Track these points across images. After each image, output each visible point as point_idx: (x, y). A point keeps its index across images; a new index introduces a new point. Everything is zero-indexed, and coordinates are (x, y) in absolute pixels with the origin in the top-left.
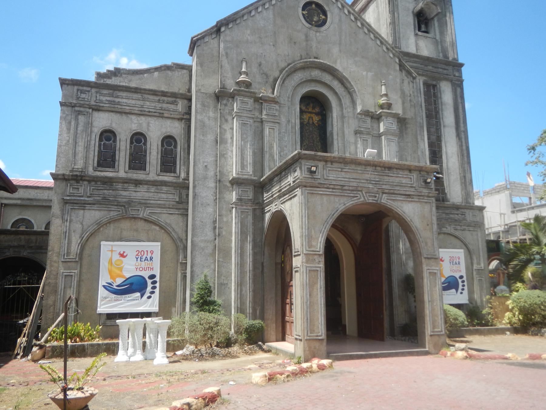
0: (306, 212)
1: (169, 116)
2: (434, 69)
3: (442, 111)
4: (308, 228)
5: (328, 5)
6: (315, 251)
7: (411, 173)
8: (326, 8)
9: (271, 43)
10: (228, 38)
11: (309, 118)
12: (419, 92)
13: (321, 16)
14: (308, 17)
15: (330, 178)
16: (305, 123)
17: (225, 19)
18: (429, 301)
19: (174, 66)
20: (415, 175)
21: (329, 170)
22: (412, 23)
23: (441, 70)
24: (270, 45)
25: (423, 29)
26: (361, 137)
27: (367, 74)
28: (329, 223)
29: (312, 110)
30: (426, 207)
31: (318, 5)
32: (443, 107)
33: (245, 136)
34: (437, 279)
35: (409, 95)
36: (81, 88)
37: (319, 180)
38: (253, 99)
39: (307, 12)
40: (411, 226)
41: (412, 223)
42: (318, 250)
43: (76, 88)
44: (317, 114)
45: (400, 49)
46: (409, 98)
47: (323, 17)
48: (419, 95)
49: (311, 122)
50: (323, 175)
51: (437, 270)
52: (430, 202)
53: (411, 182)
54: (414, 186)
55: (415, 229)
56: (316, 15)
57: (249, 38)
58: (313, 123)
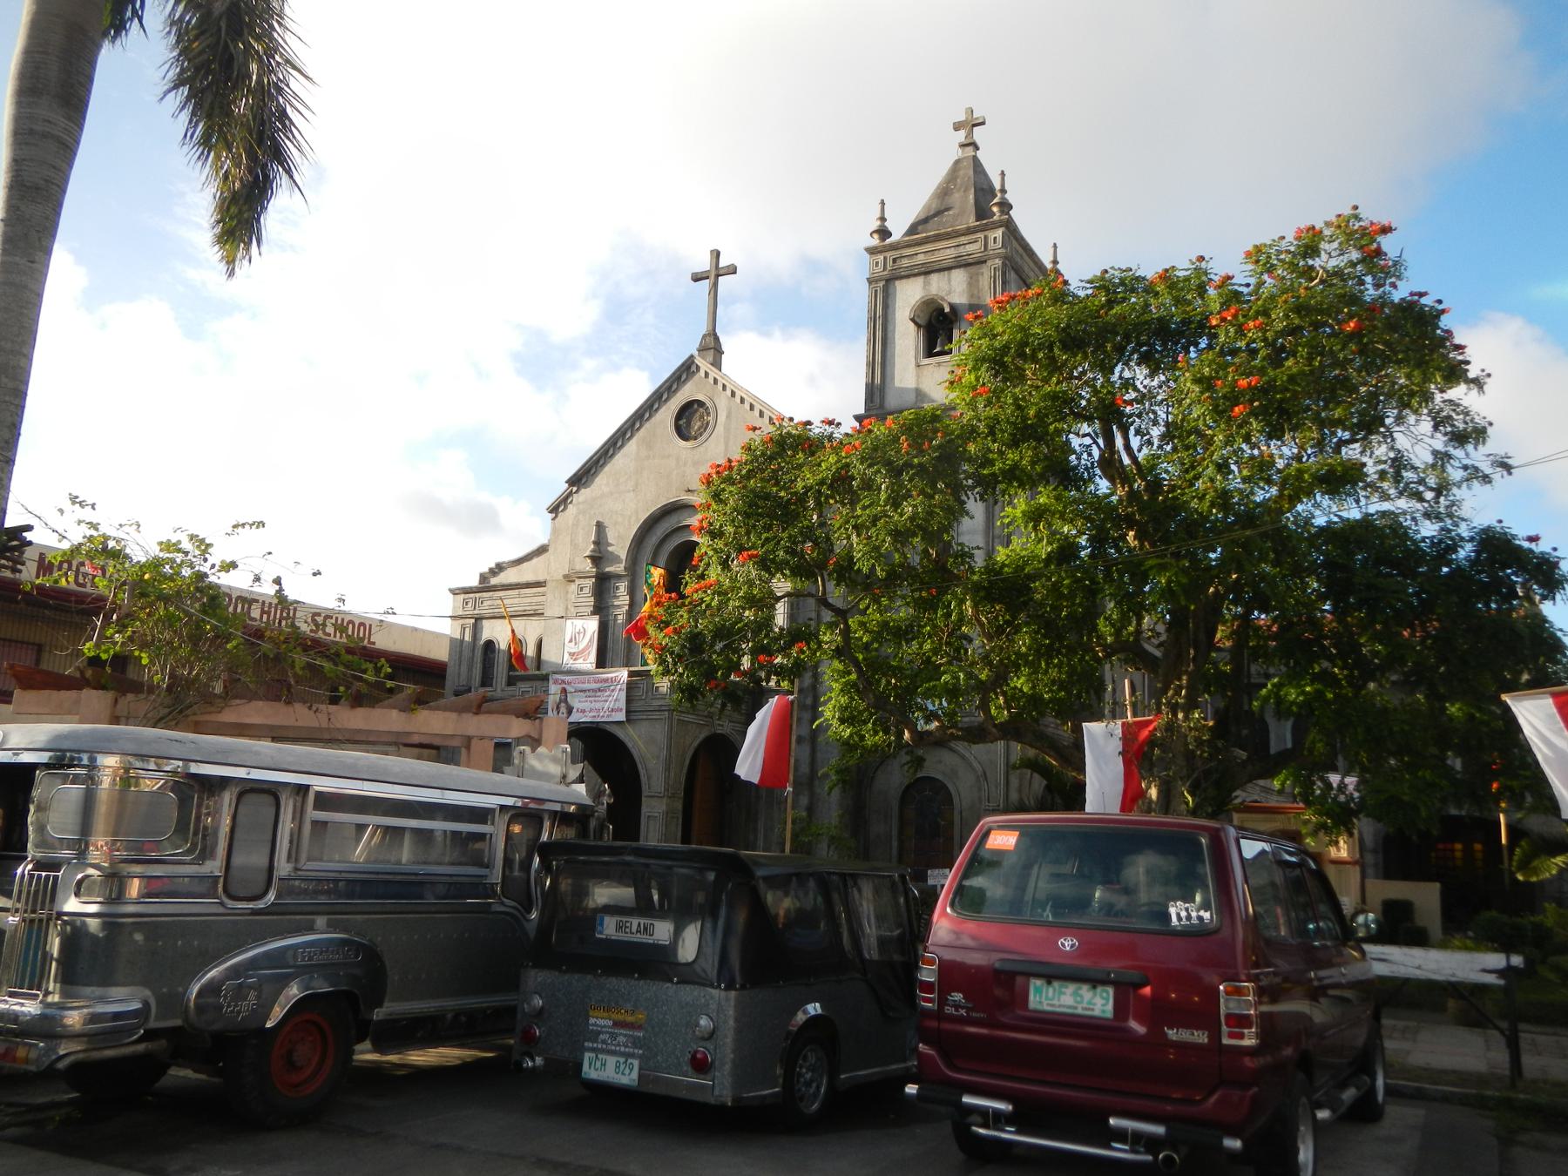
8: (708, 404)
17: (575, 475)
31: (701, 404)
36: (467, 596)
43: (462, 596)
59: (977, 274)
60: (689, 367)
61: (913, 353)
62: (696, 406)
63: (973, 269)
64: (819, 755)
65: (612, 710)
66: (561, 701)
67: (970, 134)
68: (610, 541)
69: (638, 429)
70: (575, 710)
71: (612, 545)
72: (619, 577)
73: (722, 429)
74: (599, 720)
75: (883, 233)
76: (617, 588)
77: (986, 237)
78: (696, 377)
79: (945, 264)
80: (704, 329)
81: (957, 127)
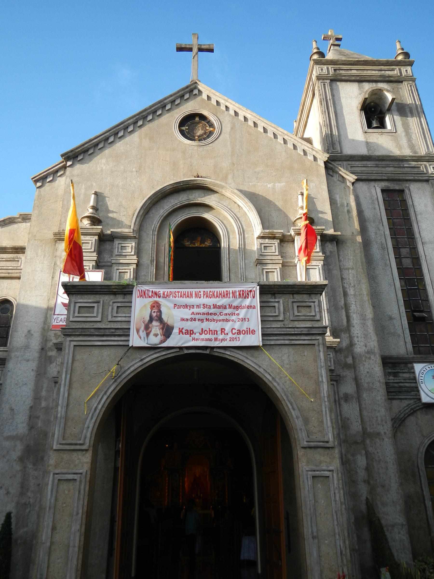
0: (68, 376)
1: (7, 275)
2: (397, 169)
4: (68, 405)
6: (76, 444)
7: (275, 298)
8: (212, 118)
9: (134, 169)
12: (376, 203)
13: (207, 128)
14: (188, 133)
15: (119, 319)
17: (72, 151)
18: (313, 538)
19: (21, 217)
20: (281, 302)
21: (118, 307)
23: (409, 170)
24: (132, 172)
26: (263, 269)
27: (274, 185)
28: (108, 393)
29: (200, 244)
30: (306, 353)
31: (202, 117)
32: (419, 217)
34: (332, 489)
37: (98, 324)
38: (96, 237)
39: (187, 127)
40: (274, 389)
41: (275, 384)
42: (81, 442)
45: (341, 152)
46: (346, 209)
47: (211, 129)
48: (377, 206)
50: (107, 316)
51: (332, 471)
52: (314, 344)
53: (275, 312)
54: (281, 319)
55: (283, 395)
56: (200, 129)
57: (104, 168)
59: (398, 89)
60: (192, 91)
61: (359, 125)
62: (197, 119)
63: (395, 85)
64: (365, 413)
65: (239, 332)
66: (151, 319)
68: (111, 209)
69: (140, 127)
70: (176, 331)
71: (113, 212)
72: (125, 238)
73: (228, 136)
74: (217, 344)
75: (321, 54)
76: (123, 248)
77: (400, 70)
78: (199, 98)
79: (375, 78)
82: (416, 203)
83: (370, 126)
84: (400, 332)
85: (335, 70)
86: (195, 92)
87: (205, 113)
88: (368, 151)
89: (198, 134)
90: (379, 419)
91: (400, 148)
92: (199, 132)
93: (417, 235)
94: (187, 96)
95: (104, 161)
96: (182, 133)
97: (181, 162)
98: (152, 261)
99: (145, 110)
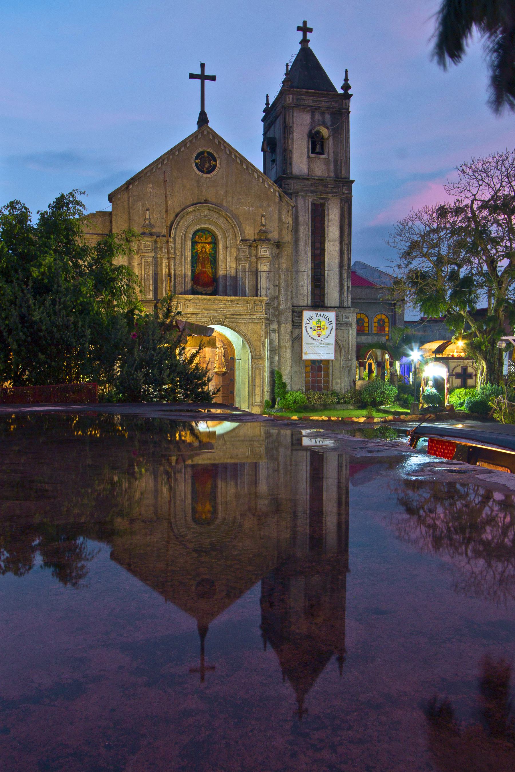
3: (328, 227)
5: (217, 153)
8: (215, 155)
10: (135, 193)
11: (202, 247)
14: (200, 165)
16: (199, 252)
22: (306, 146)
25: (318, 150)
32: (330, 223)
33: (147, 270)
35: (287, 223)
39: (199, 161)
44: (209, 243)
47: (214, 163)
48: (307, 215)
49: (203, 250)
56: (207, 162)
58: (205, 251)
61: (306, 150)
67: (305, 36)
80: (199, 111)
81: (299, 29)
82: (330, 214)
83: (313, 152)
84: (306, 293)
85: (297, 99)
86: (205, 133)
87: (211, 151)
88: (308, 172)
89: (206, 166)
90: (287, 340)
91: (328, 171)
92: (207, 165)
93: (326, 236)
94: (200, 136)
95: (151, 186)
96: (196, 164)
97: (196, 189)
98: (182, 255)
99: (174, 148)
